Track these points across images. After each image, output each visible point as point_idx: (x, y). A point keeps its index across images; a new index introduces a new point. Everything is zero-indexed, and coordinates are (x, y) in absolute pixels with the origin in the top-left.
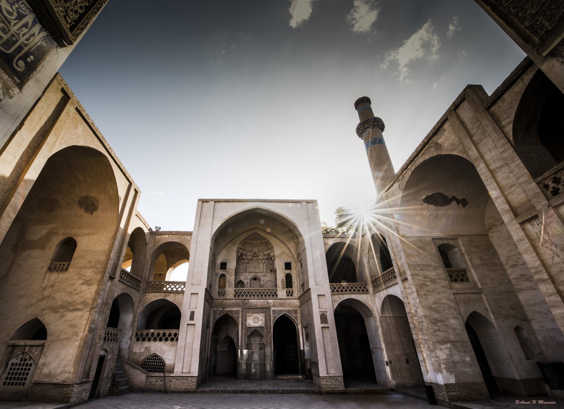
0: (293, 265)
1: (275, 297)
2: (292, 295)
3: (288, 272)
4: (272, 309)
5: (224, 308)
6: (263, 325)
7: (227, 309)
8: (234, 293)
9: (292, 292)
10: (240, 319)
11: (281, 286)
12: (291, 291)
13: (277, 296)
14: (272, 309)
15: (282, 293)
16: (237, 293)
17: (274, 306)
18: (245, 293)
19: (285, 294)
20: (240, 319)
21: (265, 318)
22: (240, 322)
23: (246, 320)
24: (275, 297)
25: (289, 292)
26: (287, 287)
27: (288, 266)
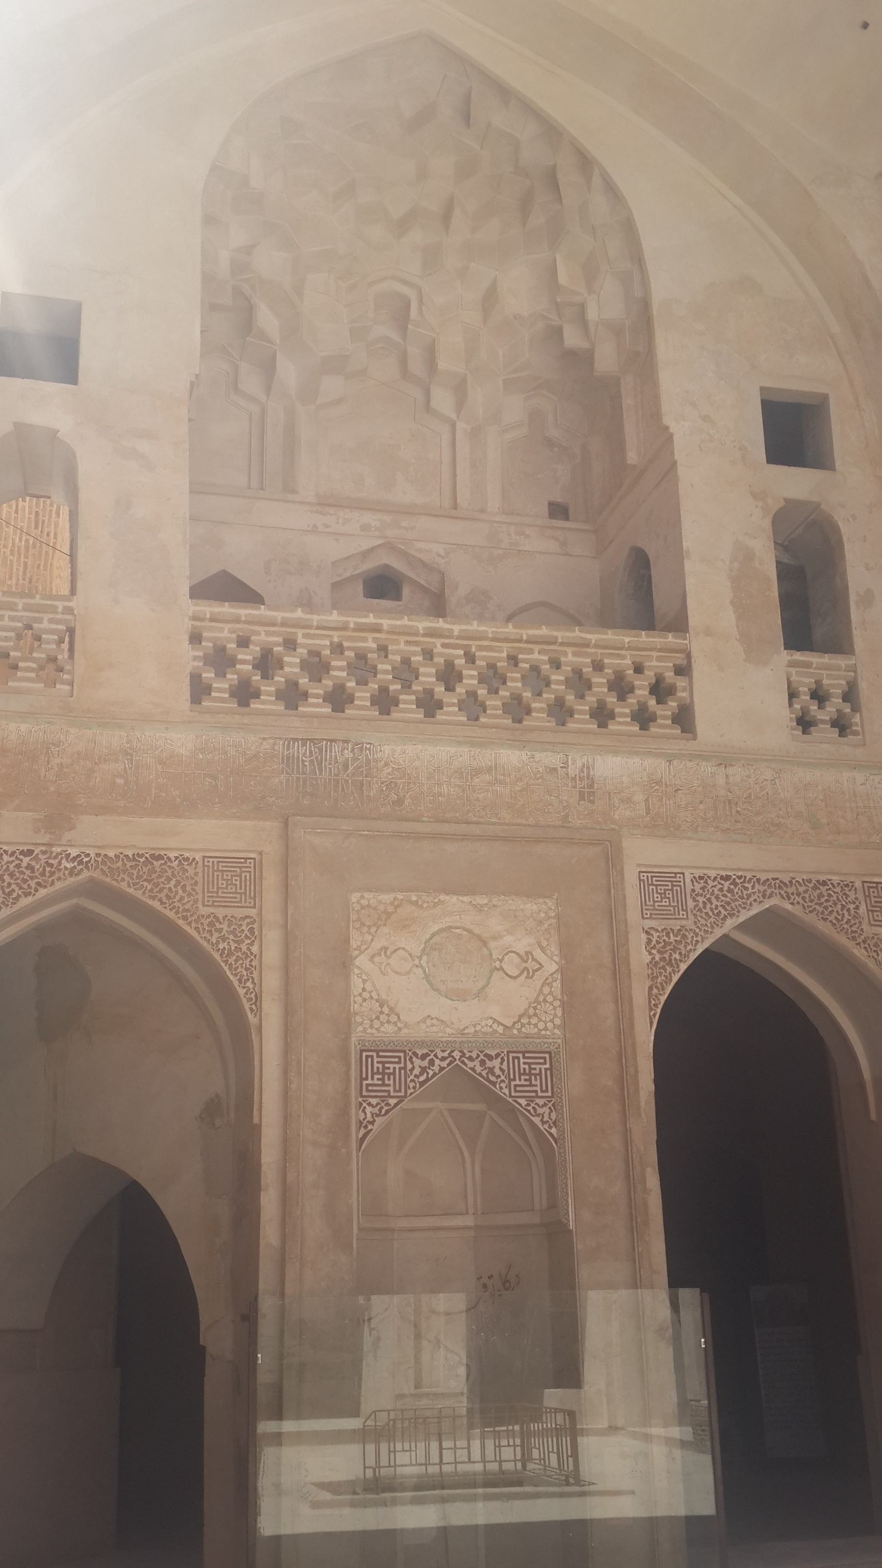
0: (845, 433)
1: (663, 726)
2: (841, 725)
3: (795, 483)
4: (642, 853)
5: (59, 816)
6: (548, 1026)
7: (101, 834)
8: (189, 658)
9: (850, 695)
10: (272, 939)
11: (728, 619)
12: (835, 685)
13: (684, 719)
14: (642, 853)
15: (742, 687)
16: (221, 660)
17: (660, 826)
18: (316, 666)
19: (781, 713)
20: (271, 952)
21: (567, 949)
22: (272, 981)
23: (342, 963)
24: (663, 726)
25: (819, 696)
26: (788, 646)
27: (792, 431)
